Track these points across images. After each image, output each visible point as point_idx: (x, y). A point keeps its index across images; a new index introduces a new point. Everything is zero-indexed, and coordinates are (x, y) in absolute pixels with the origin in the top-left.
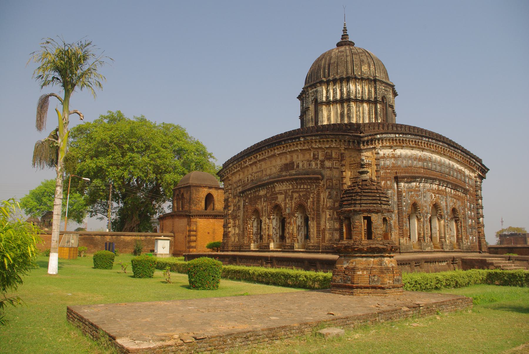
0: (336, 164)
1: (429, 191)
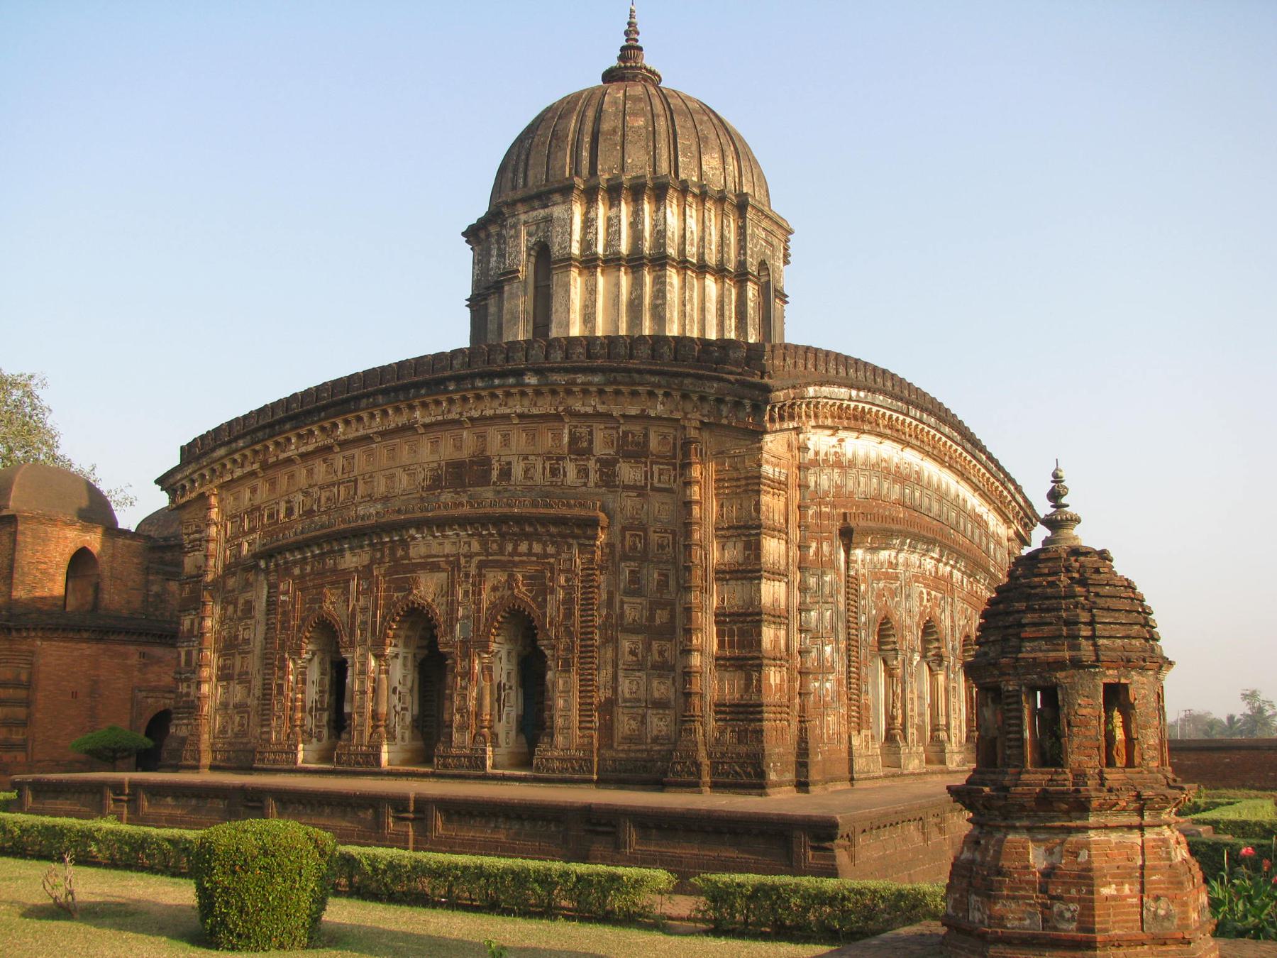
0: (661, 475)
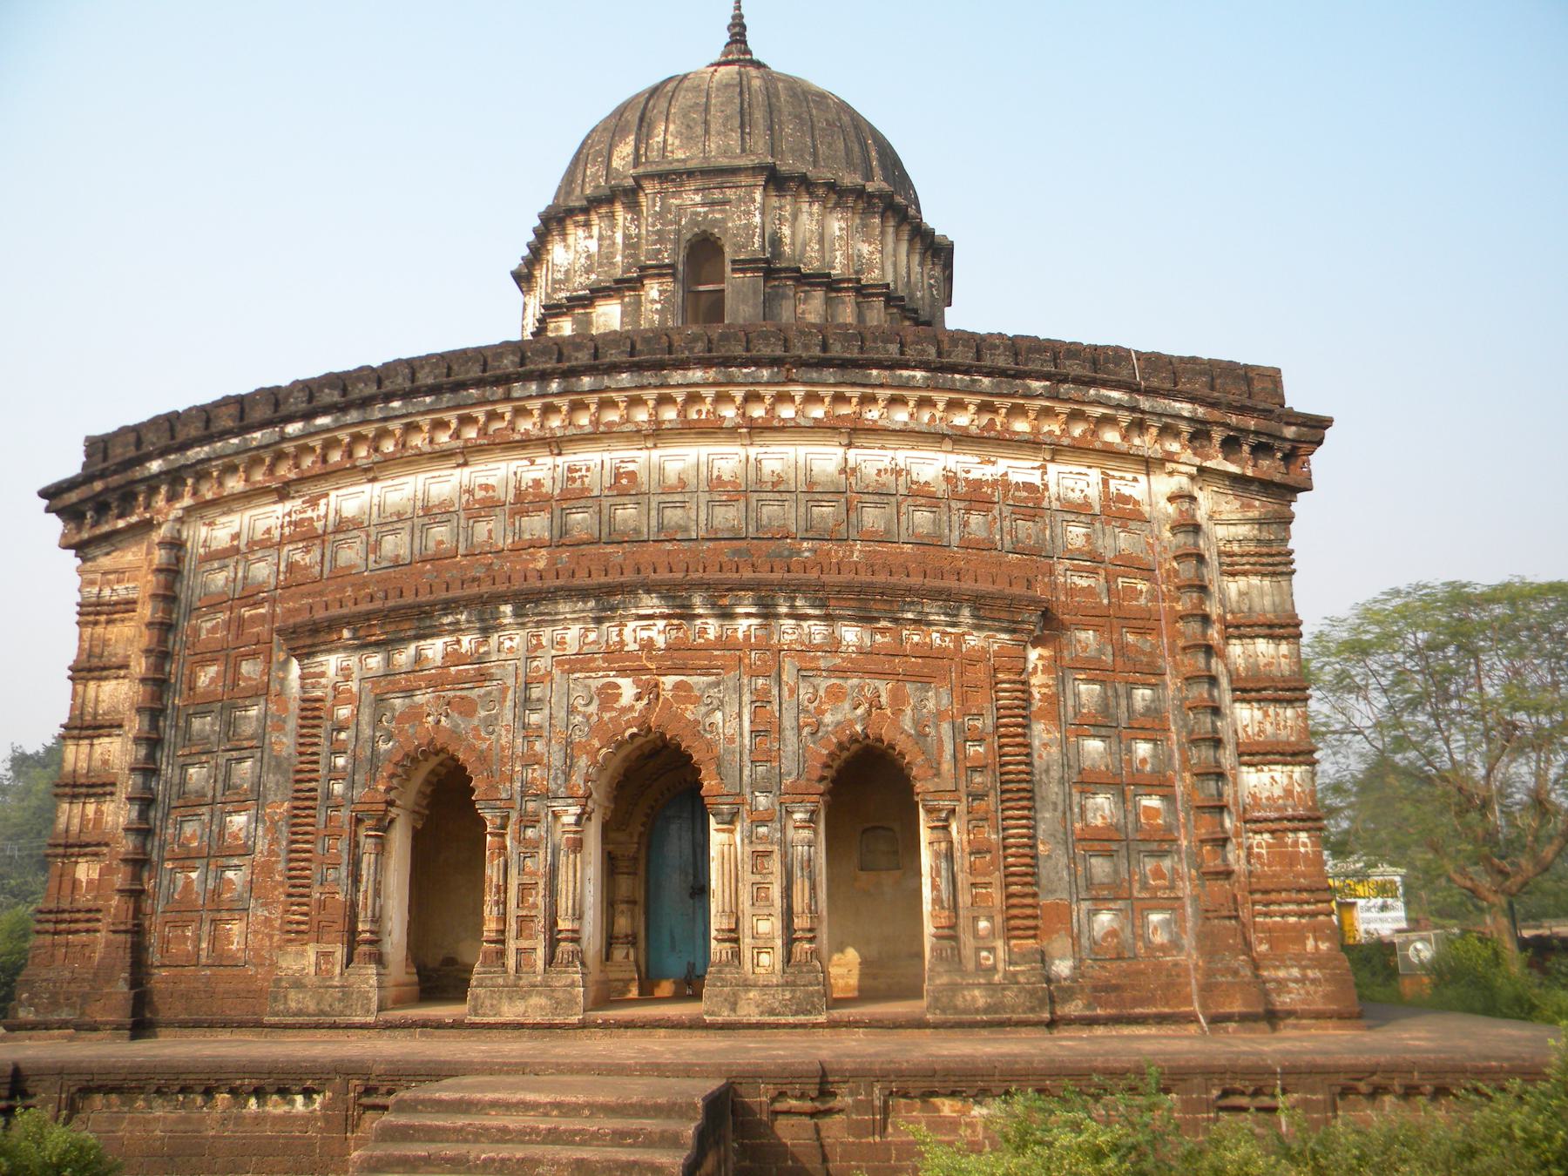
1: (578, 664)
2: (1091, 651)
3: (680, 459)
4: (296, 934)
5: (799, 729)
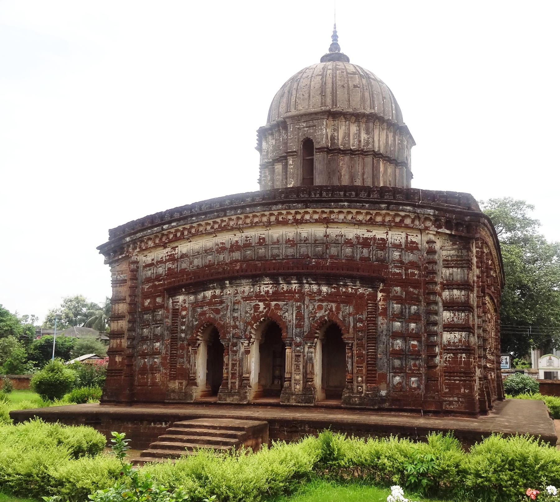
1: (247, 298)
2: (399, 294)
3: (277, 233)
4: (173, 378)
5: (310, 318)
